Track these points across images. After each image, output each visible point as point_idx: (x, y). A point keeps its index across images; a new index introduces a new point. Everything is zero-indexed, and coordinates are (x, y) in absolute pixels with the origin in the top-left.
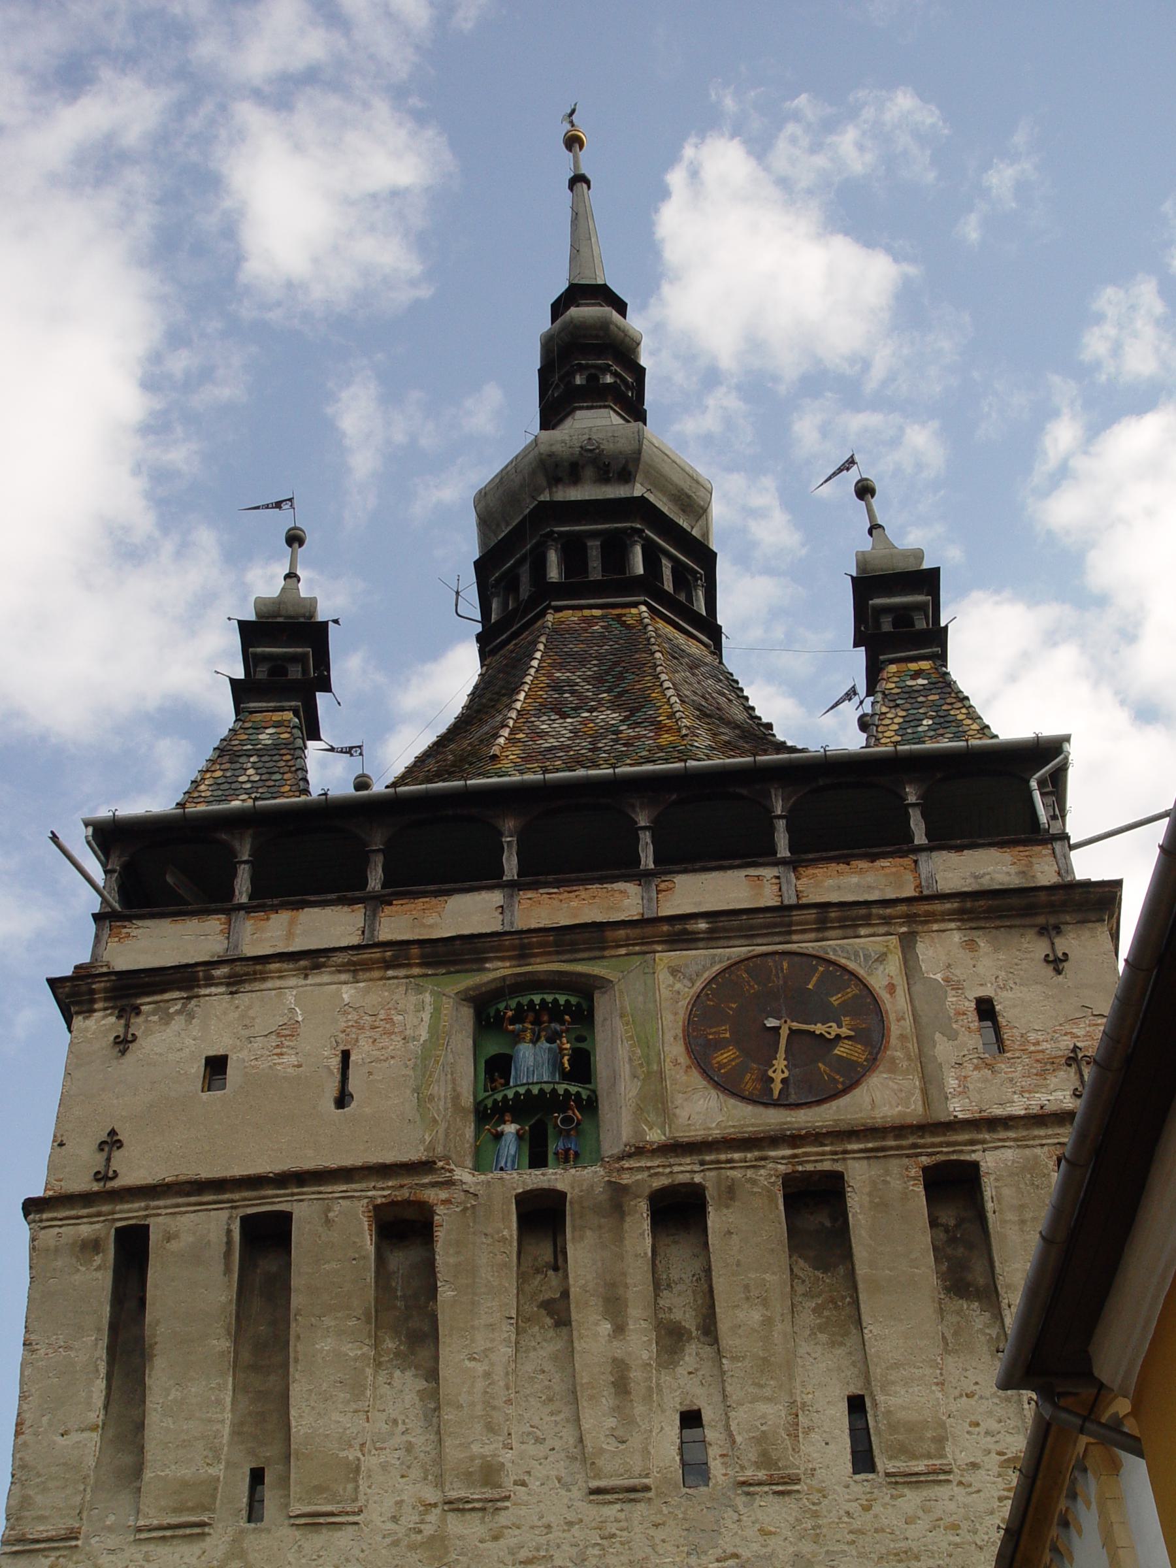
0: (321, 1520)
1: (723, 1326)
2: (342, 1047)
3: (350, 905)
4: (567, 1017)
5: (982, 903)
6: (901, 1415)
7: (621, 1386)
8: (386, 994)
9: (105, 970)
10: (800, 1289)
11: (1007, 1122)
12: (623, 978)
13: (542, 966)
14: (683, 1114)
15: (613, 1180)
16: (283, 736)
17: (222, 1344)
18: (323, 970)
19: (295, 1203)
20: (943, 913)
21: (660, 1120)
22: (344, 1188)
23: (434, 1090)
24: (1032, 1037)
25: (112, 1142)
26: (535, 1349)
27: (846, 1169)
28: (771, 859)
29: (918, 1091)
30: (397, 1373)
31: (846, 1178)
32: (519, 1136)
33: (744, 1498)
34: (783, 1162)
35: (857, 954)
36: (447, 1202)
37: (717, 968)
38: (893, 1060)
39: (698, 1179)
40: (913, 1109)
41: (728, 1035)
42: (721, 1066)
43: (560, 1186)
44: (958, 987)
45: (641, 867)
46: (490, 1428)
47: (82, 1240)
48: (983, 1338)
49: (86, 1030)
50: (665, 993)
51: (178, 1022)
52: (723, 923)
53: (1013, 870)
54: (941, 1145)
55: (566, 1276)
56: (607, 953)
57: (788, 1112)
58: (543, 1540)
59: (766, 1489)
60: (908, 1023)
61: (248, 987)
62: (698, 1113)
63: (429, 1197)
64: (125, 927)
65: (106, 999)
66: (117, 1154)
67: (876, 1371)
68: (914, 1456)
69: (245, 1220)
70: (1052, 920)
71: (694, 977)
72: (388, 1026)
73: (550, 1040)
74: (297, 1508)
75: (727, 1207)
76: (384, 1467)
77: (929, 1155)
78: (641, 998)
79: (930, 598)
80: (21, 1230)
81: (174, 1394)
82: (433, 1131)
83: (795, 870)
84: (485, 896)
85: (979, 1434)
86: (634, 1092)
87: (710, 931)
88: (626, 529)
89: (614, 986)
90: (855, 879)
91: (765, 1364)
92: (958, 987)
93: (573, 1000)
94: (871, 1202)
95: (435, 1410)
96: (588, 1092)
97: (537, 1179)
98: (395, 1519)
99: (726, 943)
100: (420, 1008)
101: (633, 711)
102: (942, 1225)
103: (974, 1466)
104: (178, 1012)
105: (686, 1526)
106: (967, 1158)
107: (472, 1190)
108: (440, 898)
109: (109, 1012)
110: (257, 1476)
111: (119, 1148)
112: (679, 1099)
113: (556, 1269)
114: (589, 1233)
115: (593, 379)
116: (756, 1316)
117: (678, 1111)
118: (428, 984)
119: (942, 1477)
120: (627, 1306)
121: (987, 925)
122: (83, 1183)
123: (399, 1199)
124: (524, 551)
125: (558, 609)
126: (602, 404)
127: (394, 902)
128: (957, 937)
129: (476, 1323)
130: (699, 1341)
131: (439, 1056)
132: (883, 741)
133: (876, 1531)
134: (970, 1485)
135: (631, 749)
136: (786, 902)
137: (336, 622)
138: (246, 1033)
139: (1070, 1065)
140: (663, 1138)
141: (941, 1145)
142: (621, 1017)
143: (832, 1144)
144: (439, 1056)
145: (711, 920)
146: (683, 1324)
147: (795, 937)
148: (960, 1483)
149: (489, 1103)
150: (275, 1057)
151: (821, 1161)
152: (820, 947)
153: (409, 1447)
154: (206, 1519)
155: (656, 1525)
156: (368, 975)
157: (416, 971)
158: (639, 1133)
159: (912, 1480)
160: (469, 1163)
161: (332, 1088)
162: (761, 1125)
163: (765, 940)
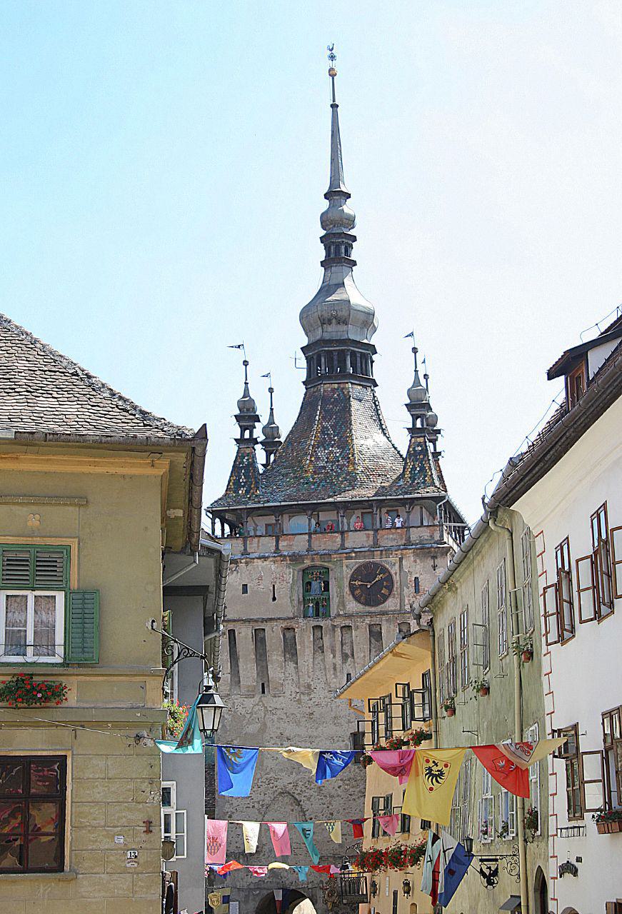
1: (355, 657)
7: (335, 669)
10: (372, 646)
13: (318, 563)
14: (348, 607)
36: (297, 628)
46: (309, 677)
51: (235, 572)
60: (399, 584)
76: (288, 684)
90: (391, 536)
92: (411, 573)
101: (343, 448)
110: (263, 684)
132: (406, 476)
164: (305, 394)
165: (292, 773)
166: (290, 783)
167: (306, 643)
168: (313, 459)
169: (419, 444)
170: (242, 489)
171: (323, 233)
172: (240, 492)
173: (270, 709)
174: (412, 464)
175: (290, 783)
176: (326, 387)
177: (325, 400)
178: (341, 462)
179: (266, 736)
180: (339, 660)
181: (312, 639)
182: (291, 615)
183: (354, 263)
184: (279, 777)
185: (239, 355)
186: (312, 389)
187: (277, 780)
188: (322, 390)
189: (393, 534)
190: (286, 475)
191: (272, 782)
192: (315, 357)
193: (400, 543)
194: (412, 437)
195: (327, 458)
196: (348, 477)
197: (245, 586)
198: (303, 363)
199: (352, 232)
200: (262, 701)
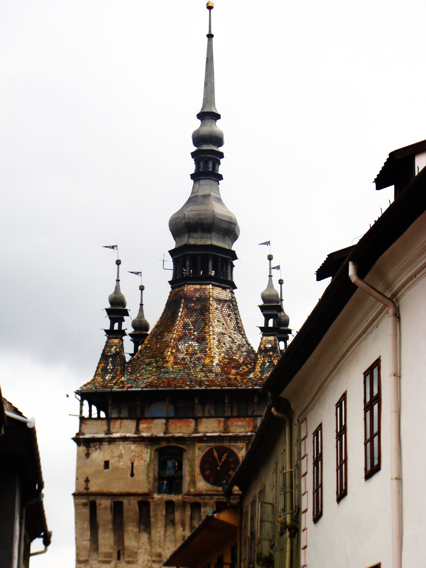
2: (132, 461)
13: (173, 444)
17: (110, 526)
25: (87, 481)
32: (167, 484)
37: (208, 449)
39: (200, 501)
41: (208, 467)
46: (160, 547)
50: (197, 454)
51: (98, 450)
66: (89, 484)
74: (127, 559)
80: (71, 499)
81: (103, 536)
88: (208, 254)
90: (240, 423)
100: (147, 453)
104: (99, 448)
112: (197, 482)
122: (82, 490)
132: (256, 370)
138: (113, 455)
142: (188, 459)
153: (146, 549)
157: (147, 443)
158: (189, 490)
160: (156, 492)
161: (130, 472)
164: (171, 293)
167: (160, 517)
168: (174, 351)
169: (270, 342)
170: (109, 375)
171: (194, 149)
172: (107, 378)
174: (262, 359)
176: (189, 288)
177: (188, 299)
178: (199, 355)
181: (164, 513)
183: (220, 177)
185: (113, 255)
186: (177, 290)
188: (185, 290)
189: (242, 421)
190: (149, 364)
193: (248, 430)
194: (263, 335)
195: (187, 351)
196: (204, 369)
197: (107, 464)
198: (170, 263)
199: (220, 149)
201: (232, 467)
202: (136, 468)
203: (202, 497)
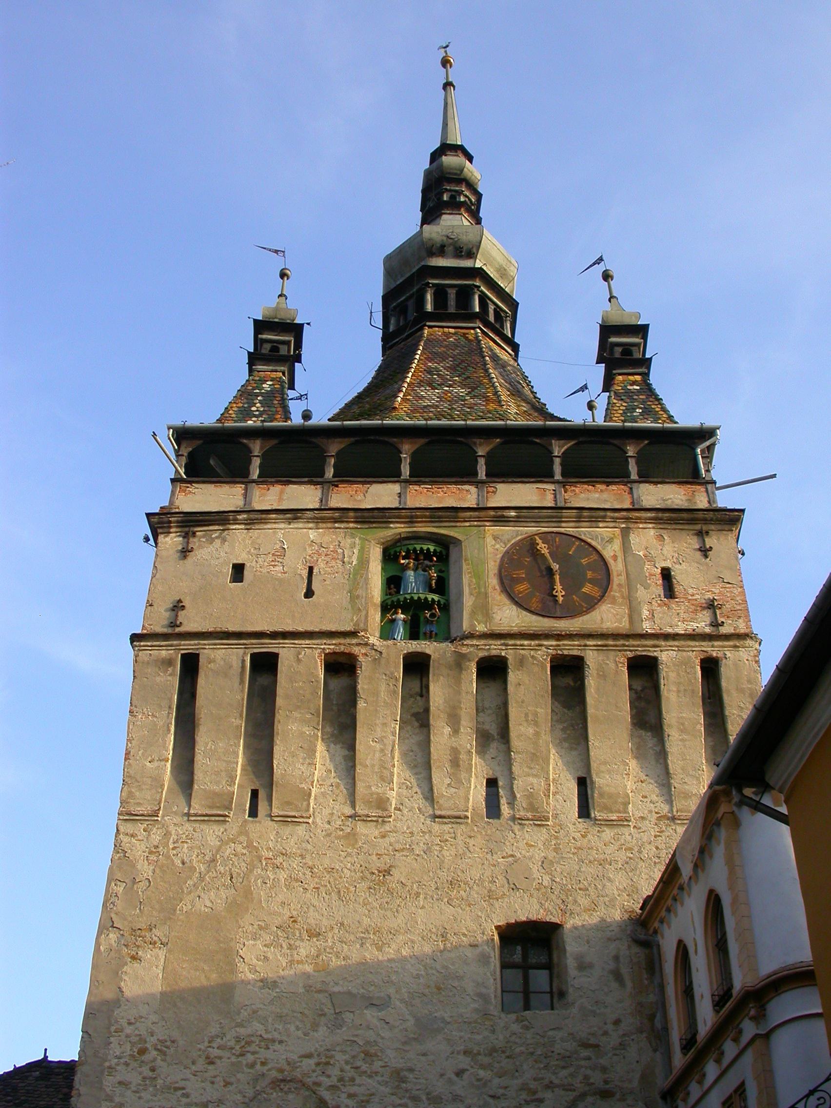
0: (289, 820)
2: (308, 564)
3: (314, 485)
4: (435, 559)
5: (667, 515)
6: (606, 789)
8: (334, 537)
9: (177, 510)
11: (675, 637)
12: (467, 539)
15: (457, 650)
16: (276, 386)
18: (299, 520)
19: (280, 649)
20: (646, 519)
21: (485, 619)
22: (307, 642)
23: (360, 592)
24: (691, 591)
25: (178, 607)
26: (408, 738)
27: (586, 655)
28: (551, 480)
29: (626, 616)
30: (332, 745)
31: (585, 660)
33: (518, 826)
34: (551, 648)
35: (597, 537)
37: (520, 538)
38: (614, 597)
39: (503, 654)
40: (623, 625)
42: (521, 593)
43: (428, 651)
44: (651, 560)
45: (479, 478)
46: (382, 779)
47: (162, 659)
48: (651, 751)
49: (166, 543)
50: (490, 549)
51: (218, 541)
52: (524, 513)
53: (684, 498)
54: (638, 646)
55: (428, 700)
56: (458, 524)
57: (555, 621)
58: (409, 840)
59: (531, 822)
60: (623, 577)
61: (257, 527)
62: (506, 618)
63: (355, 651)
64: (188, 487)
65: (177, 527)
66: (182, 614)
67: (594, 765)
68: (612, 812)
69: (253, 656)
70: (705, 528)
71: (506, 541)
72: (335, 554)
73: (424, 570)
75: (519, 670)
76: (324, 794)
77: (631, 651)
78: (476, 551)
79: (642, 340)
80: (129, 652)
82: (358, 615)
83: (564, 486)
84: (390, 486)
85: (647, 802)
86: (471, 603)
87: (517, 517)
89: (461, 543)
91: (534, 757)
93: (438, 549)
94: (598, 674)
95: (352, 767)
96: (444, 601)
97: (415, 646)
98: (329, 823)
99: (525, 524)
100: (353, 546)
101: (473, 389)
102: (634, 689)
103: (642, 818)
105: (487, 838)
106: (651, 654)
107: (379, 650)
108: (365, 486)
109: (178, 534)
110: (255, 794)
111: (183, 610)
113: (422, 696)
114: (441, 678)
115: (453, 197)
116: (531, 731)
117: (494, 615)
118: (358, 534)
119: (625, 823)
120: (461, 719)
121: (669, 527)
123: (338, 651)
124: (411, 292)
125: (430, 327)
126: (457, 212)
127: (340, 486)
128: (652, 532)
129: (378, 722)
130: (498, 741)
131: (363, 574)
133: (589, 849)
134: (640, 828)
135: (472, 410)
136: (559, 505)
137: (308, 324)
139: (710, 609)
140: (486, 629)
141: (638, 646)
142: (465, 561)
143: (578, 640)
144: (363, 574)
145: (518, 511)
146: (490, 731)
147: (563, 525)
148: (635, 827)
149: (389, 602)
150: (271, 567)
151: (572, 649)
152: (577, 531)
154: (227, 814)
155: (470, 837)
156: (324, 525)
157: (351, 525)
158: (473, 626)
159: (609, 823)
160: (378, 634)
162: (541, 627)
163: (546, 525)
165: (315, 1026)
166: (309, 1056)
169: (634, 383)
170: (254, 419)
173: (265, 853)
175: (309, 1056)
179: (248, 921)
180: (467, 739)
182: (348, 628)
184: (276, 1035)
185: (278, 263)
187: (268, 1043)
191: (253, 1047)
192: (411, 304)
197: (238, 571)
200: (247, 834)
201: (589, 577)
202: (321, 578)
203: (511, 642)
